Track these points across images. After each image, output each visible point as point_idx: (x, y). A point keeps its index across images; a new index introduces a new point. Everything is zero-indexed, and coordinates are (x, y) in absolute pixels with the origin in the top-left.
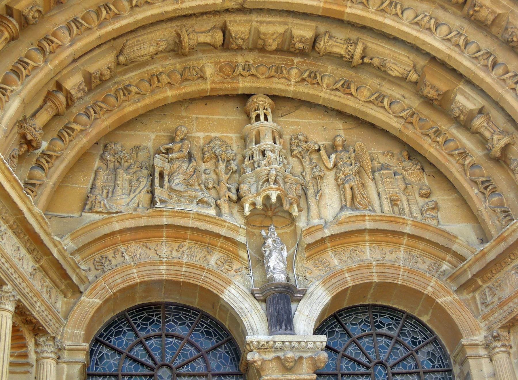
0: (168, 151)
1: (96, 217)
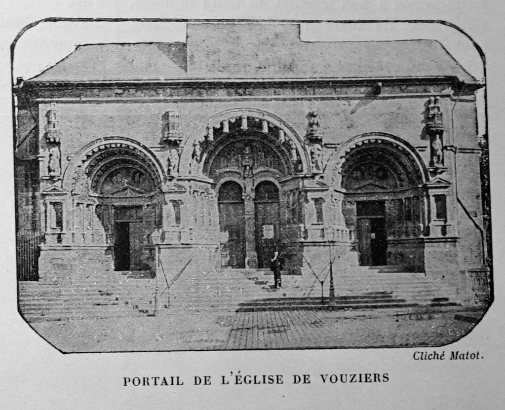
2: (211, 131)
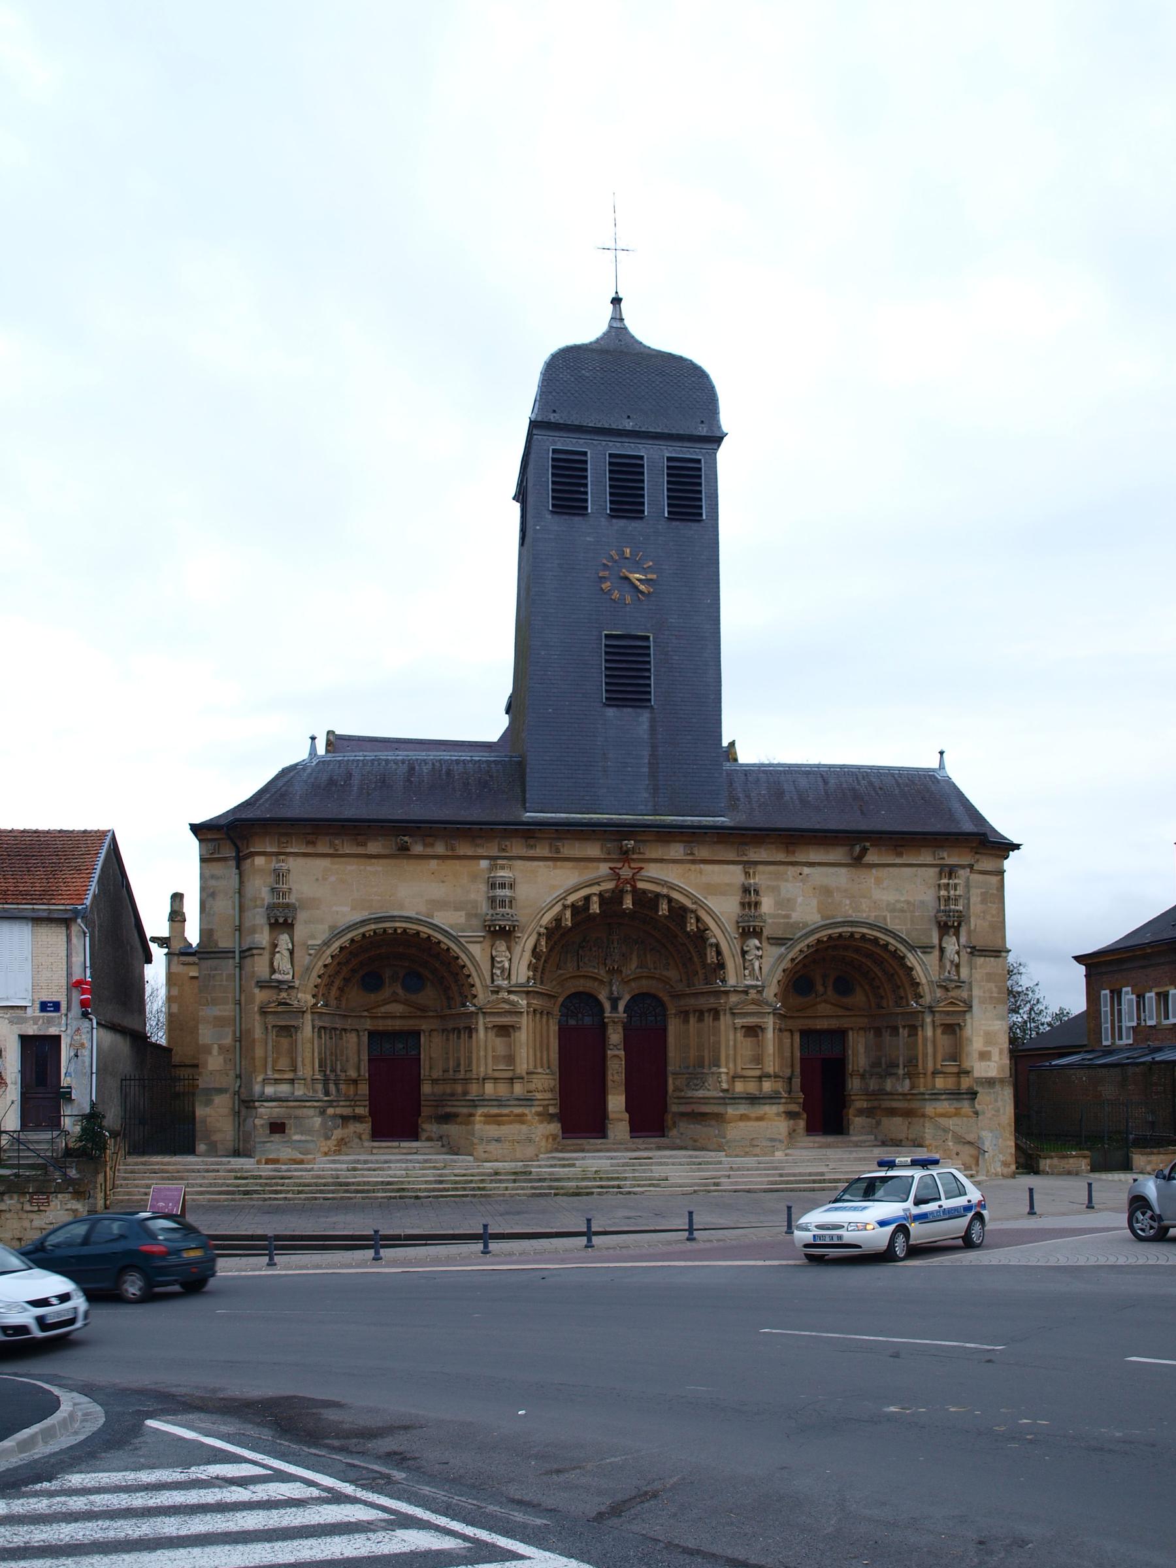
0: (583, 947)
1: (561, 972)
2: (568, 914)
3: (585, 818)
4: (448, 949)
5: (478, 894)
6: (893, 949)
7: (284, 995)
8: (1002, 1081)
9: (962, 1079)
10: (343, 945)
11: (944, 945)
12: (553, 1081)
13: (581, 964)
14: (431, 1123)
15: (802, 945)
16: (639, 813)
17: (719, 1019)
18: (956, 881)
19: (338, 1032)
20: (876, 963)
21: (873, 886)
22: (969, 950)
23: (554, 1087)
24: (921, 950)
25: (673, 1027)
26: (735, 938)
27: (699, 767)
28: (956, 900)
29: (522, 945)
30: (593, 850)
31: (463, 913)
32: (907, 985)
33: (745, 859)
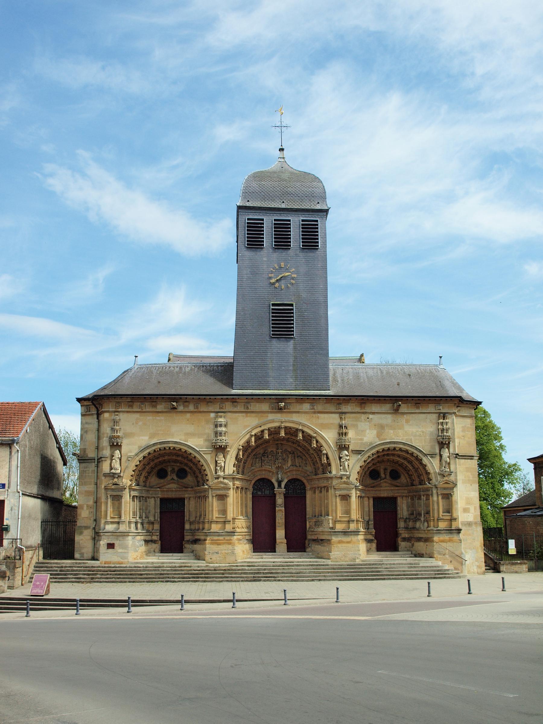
0: (264, 456)
1: (254, 468)
2: (253, 439)
3: (261, 392)
4: (195, 457)
5: (209, 429)
6: (415, 455)
7: (116, 480)
8: (476, 523)
9: (453, 523)
10: (145, 456)
11: (442, 453)
12: (249, 523)
13: (263, 464)
14: (189, 544)
15: (369, 454)
16: (288, 389)
17: (328, 491)
18: (447, 421)
19: (144, 498)
20: (409, 463)
21: (404, 423)
22: (455, 456)
23: (249, 526)
24: (430, 456)
25: (309, 495)
26: (335, 450)
27: (317, 366)
28: (447, 430)
29: (230, 455)
30: (265, 407)
31: (202, 439)
32: (424, 474)
33: (340, 411)
